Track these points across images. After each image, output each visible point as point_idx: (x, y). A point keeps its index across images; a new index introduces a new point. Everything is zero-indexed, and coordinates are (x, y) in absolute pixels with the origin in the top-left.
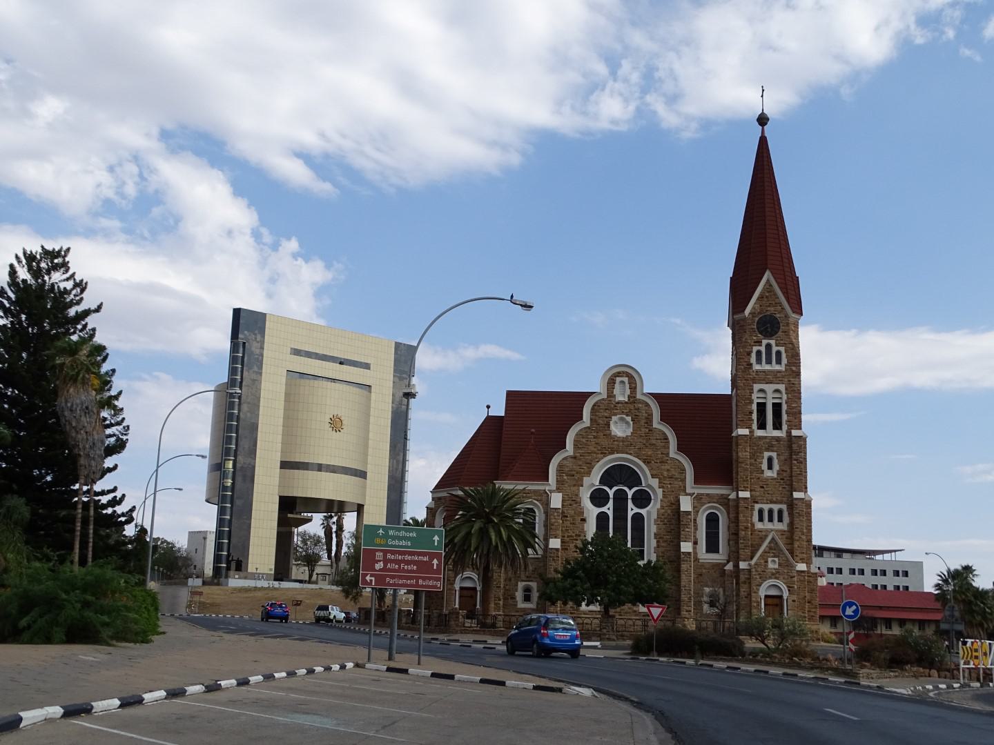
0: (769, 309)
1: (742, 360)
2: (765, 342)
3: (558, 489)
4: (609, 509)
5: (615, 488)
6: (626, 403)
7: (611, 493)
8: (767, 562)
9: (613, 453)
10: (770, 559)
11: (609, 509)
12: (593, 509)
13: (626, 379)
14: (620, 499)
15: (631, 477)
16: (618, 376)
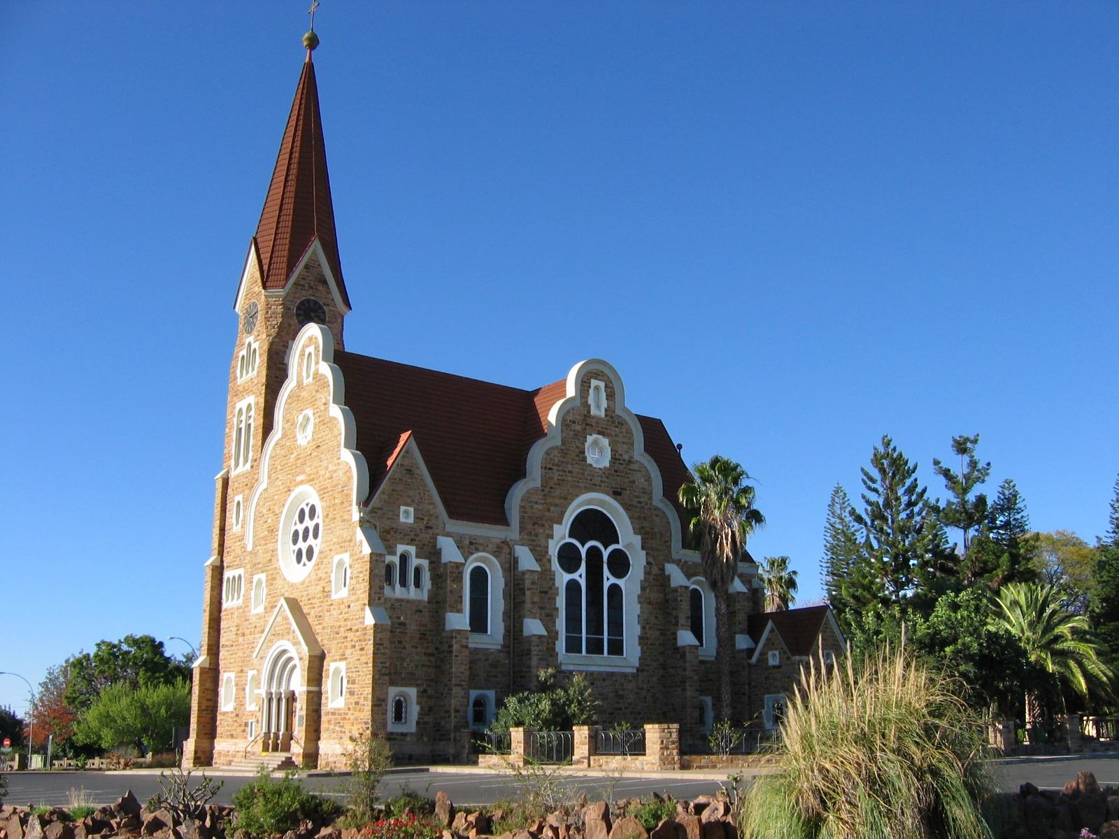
3: (522, 539)
4: (580, 576)
7: (583, 551)
11: (580, 576)
12: (562, 575)
13: (602, 385)
15: (607, 532)
16: (592, 377)
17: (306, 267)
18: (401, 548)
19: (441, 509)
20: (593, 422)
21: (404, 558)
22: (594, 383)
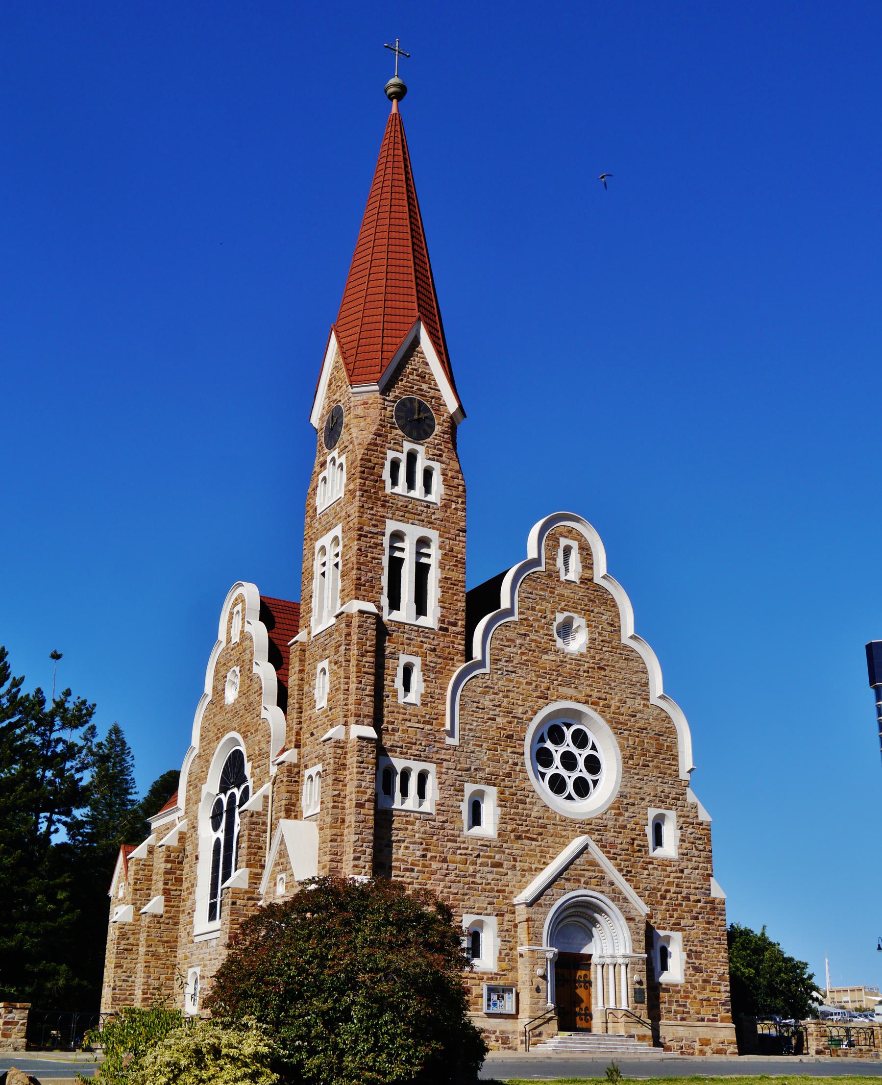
0: (335, 397)
1: (308, 508)
2: (329, 459)
3: (186, 813)
5: (229, 792)
6: (238, 645)
8: (275, 885)
9: (223, 736)
10: (279, 877)
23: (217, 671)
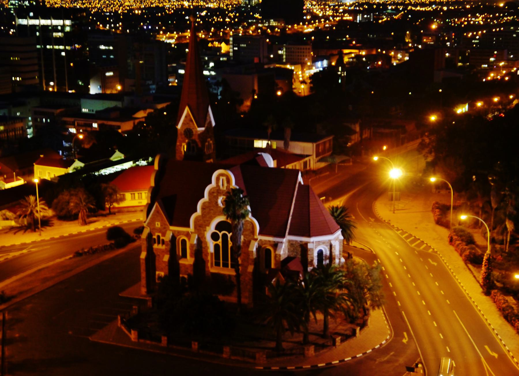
7: (220, 234)
13: (225, 178)
14: (225, 236)
17: (186, 117)
18: (157, 234)
19: (167, 223)
20: (221, 192)
21: (158, 237)
22: (221, 178)
23: (211, 193)
